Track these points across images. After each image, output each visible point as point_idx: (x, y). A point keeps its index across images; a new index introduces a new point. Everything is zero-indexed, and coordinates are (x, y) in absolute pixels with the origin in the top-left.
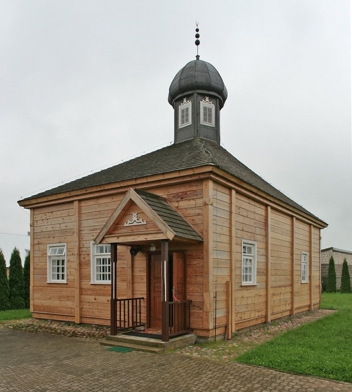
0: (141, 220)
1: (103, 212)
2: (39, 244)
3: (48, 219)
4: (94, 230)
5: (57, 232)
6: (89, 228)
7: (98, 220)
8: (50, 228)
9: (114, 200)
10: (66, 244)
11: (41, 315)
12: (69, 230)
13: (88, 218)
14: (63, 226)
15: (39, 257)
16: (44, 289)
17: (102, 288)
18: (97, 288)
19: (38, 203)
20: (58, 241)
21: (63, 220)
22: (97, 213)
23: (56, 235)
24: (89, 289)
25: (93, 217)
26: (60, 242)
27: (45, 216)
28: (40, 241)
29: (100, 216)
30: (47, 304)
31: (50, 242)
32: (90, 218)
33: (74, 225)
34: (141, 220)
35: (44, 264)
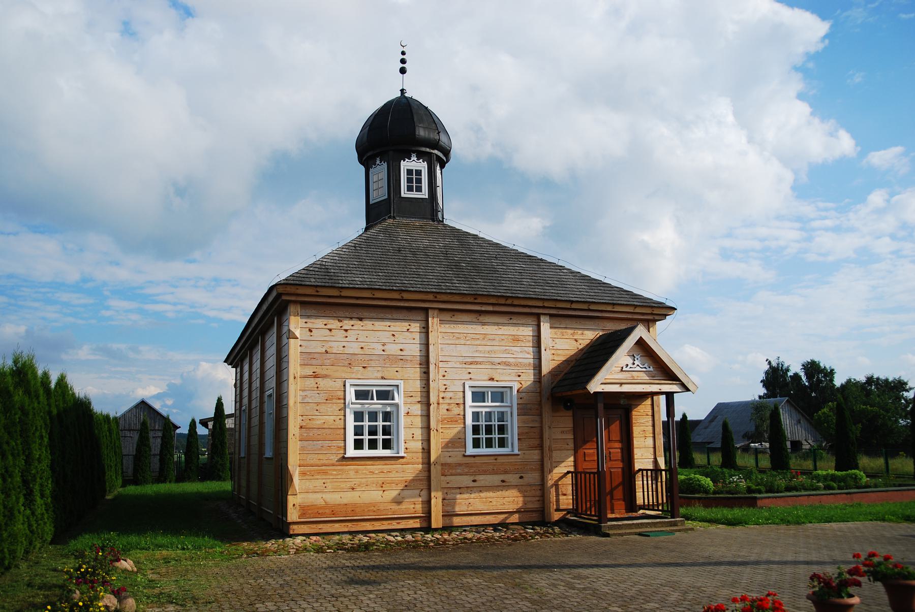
0: (646, 366)
1: (491, 337)
2: (316, 376)
3: (346, 330)
4: (471, 363)
5: (374, 358)
6: (461, 359)
7: (480, 348)
8: (353, 348)
9: (515, 321)
10: (402, 382)
11: (321, 526)
12: (409, 358)
13: (457, 342)
14: (393, 349)
15: (318, 404)
16: (335, 470)
17: (491, 460)
18: (477, 460)
19: (357, 298)
20: (380, 375)
21: (393, 338)
22: (478, 336)
23: (373, 363)
24: (460, 465)
25: (468, 342)
26: (383, 378)
27: (340, 324)
28: (319, 371)
29: (483, 343)
30: (345, 501)
31: (353, 376)
32: (463, 342)
33: (414, 349)
34: (646, 366)
35: (332, 418)
